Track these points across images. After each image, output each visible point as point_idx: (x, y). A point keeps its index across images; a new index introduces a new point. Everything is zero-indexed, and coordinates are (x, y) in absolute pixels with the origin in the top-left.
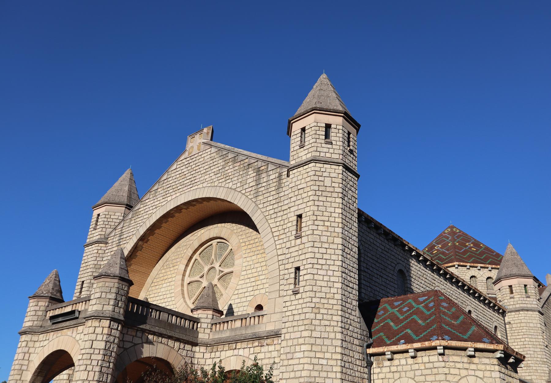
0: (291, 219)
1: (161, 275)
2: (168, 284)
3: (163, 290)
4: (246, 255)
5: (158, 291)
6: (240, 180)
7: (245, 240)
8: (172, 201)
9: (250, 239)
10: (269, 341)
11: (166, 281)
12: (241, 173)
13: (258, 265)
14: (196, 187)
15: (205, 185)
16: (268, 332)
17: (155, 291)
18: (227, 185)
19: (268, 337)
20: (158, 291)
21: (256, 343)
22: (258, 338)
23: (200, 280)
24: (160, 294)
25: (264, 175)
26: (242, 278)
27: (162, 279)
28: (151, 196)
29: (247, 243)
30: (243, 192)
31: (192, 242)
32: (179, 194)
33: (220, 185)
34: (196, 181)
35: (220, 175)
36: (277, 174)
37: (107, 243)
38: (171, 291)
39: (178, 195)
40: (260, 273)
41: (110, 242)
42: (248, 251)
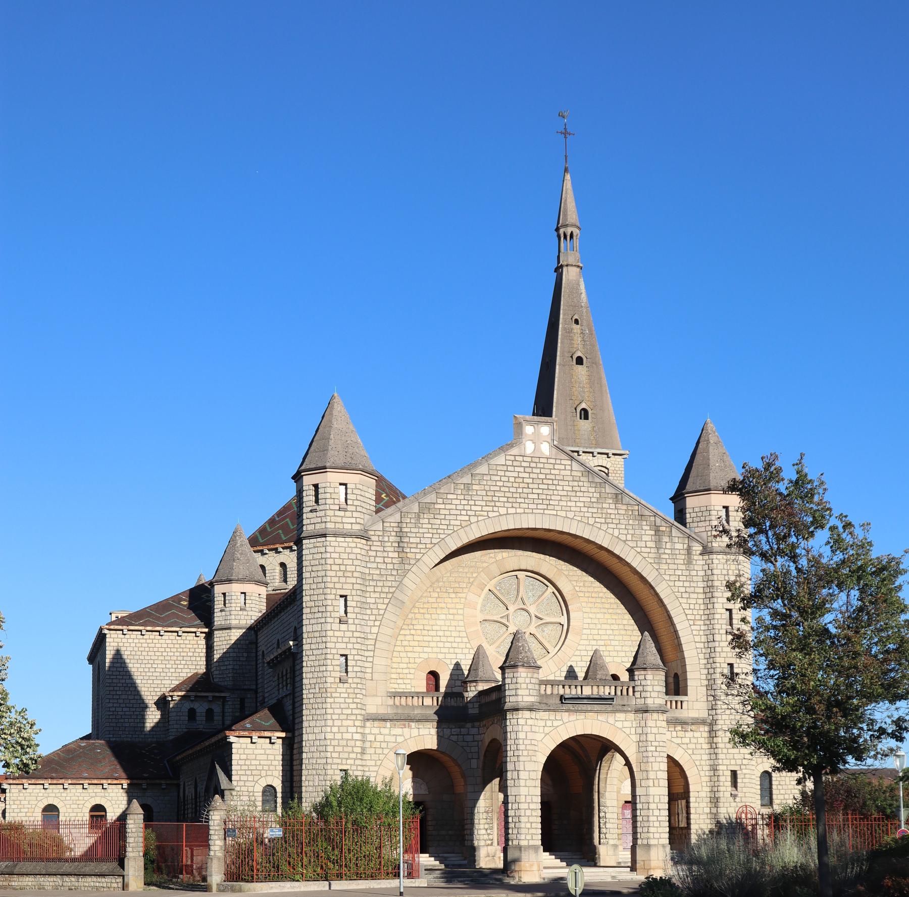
0: (719, 611)
1: (431, 600)
2: (451, 617)
3: (439, 623)
4: (588, 610)
5: (432, 622)
6: (631, 532)
7: (583, 589)
8: (510, 518)
9: (591, 590)
10: (693, 727)
11: (446, 611)
12: (631, 522)
13: (608, 627)
14: (555, 513)
15: (571, 515)
16: (693, 719)
17: (425, 622)
18: (610, 531)
19: (693, 724)
20: (432, 622)
21: (679, 728)
22: (683, 723)
23: (504, 621)
24: (435, 628)
25: (666, 539)
26: (585, 637)
27: (435, 605)
28: (459, 492)
29: (587, 595)
30: (638, 550)
31: (486, 565)
32: (521, 511)
33: (598, 525)
34: (551, 502)
35: (595, 510)
36: (686, 546)
37: (368, 539)
38: (458, 629)
39: (519, 511)
40: (612, 637)
41: (373, 538)
42: (590, 605)
